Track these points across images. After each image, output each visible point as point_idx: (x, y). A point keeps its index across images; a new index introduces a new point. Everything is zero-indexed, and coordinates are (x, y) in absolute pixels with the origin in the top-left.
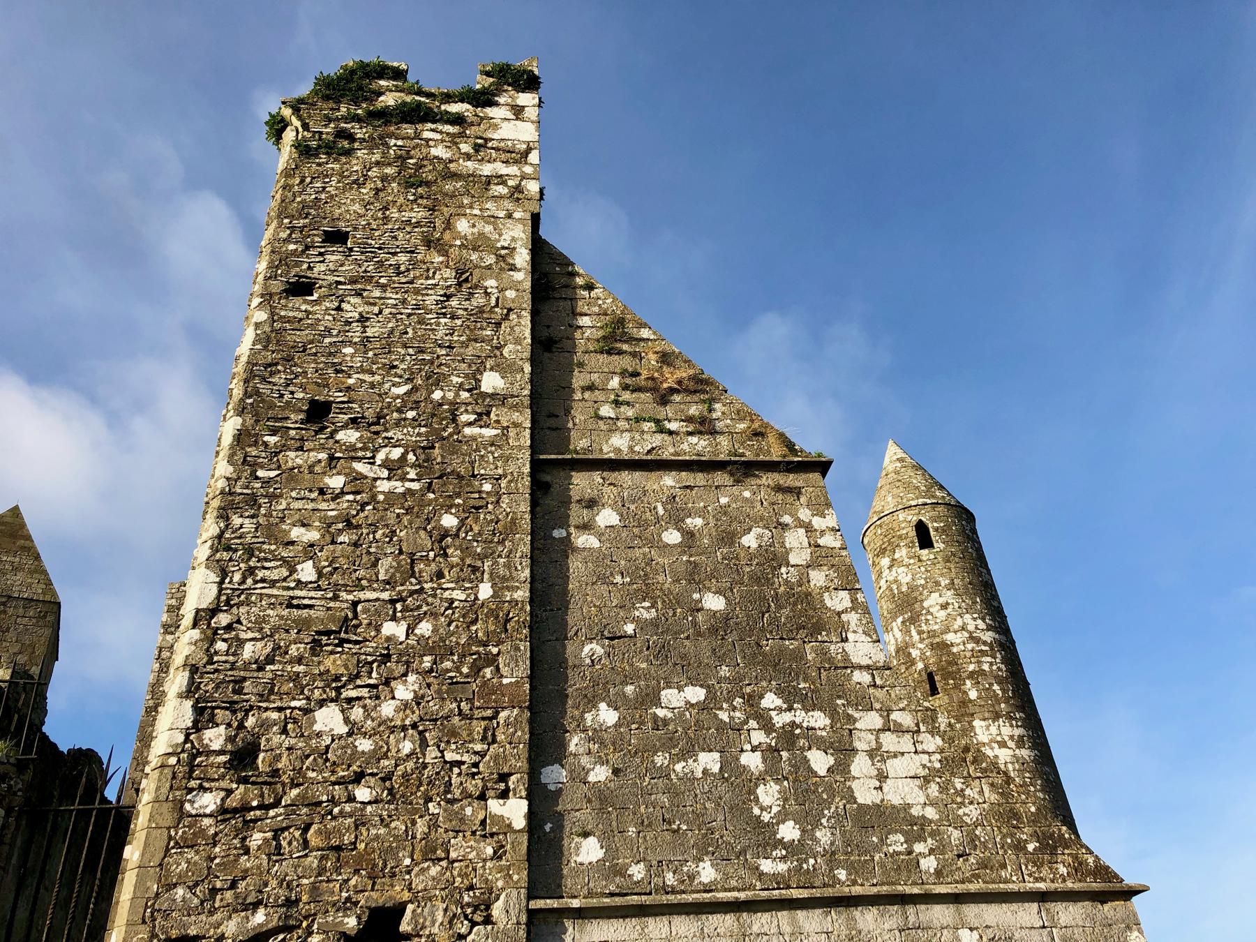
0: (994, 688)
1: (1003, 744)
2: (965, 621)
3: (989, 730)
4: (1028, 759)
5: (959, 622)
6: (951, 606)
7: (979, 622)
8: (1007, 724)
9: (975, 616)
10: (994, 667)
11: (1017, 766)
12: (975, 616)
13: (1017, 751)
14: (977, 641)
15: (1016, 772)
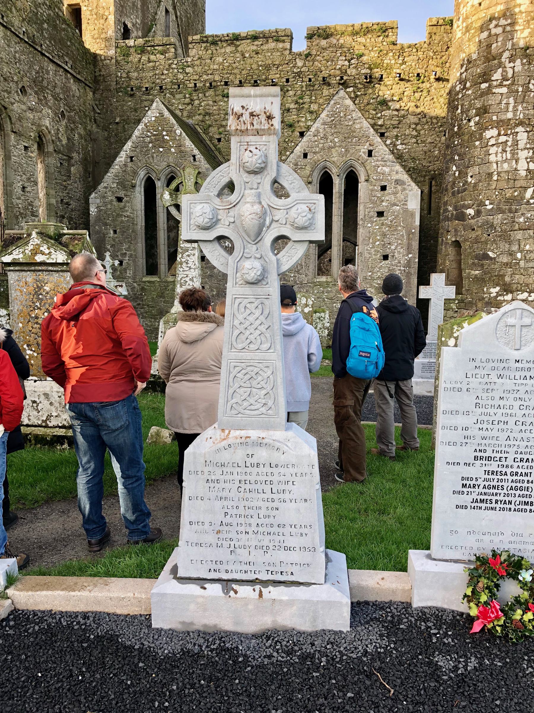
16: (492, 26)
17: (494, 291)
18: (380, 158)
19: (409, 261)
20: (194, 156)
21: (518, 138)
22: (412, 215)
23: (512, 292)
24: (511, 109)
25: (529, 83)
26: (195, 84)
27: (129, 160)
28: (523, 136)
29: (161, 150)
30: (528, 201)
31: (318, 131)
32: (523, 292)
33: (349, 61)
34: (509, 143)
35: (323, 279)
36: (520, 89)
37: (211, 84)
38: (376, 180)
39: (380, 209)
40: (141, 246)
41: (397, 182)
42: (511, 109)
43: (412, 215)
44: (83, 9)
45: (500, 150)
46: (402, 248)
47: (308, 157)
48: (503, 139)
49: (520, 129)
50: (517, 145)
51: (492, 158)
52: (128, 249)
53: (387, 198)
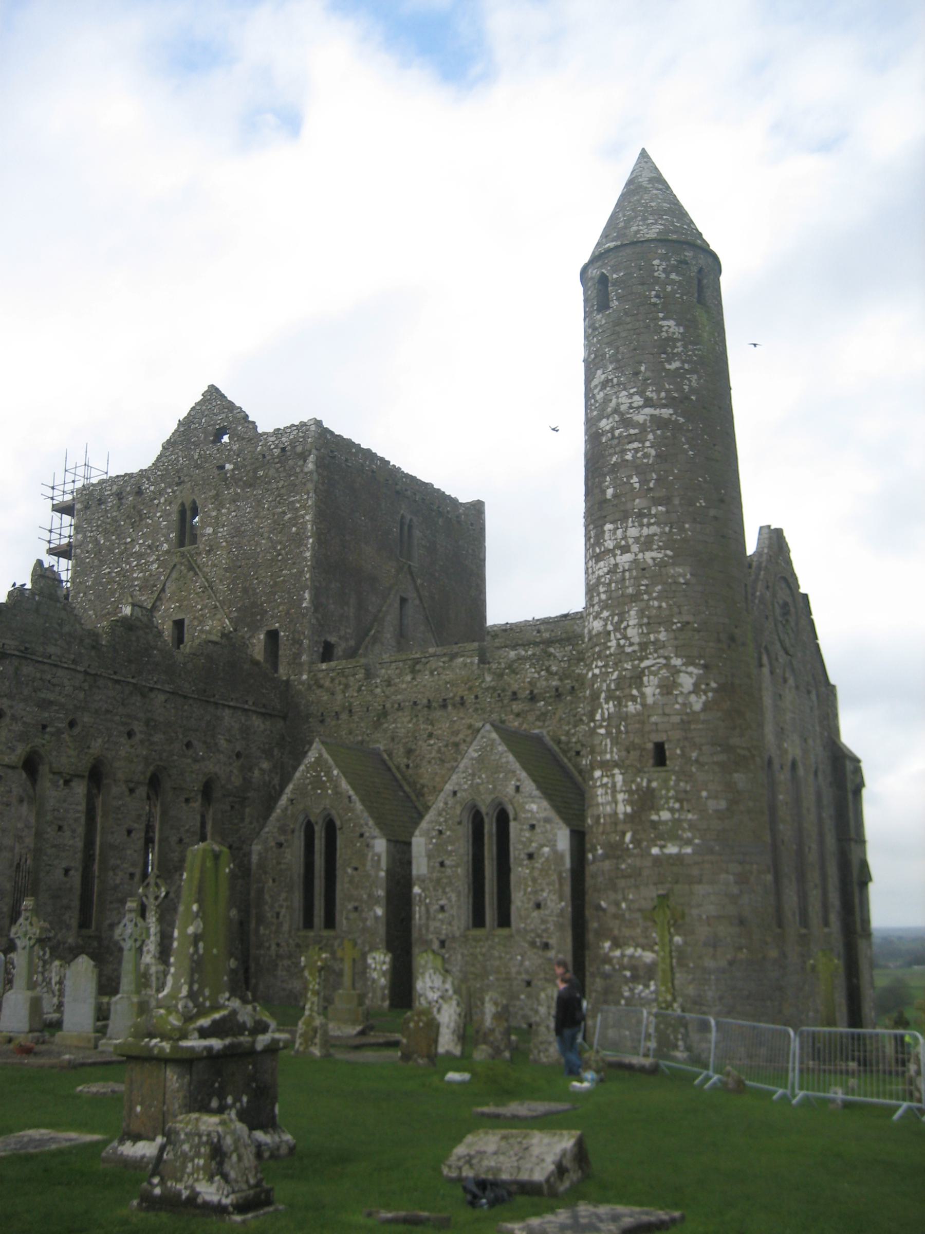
0: (632, 481)
1: (626, 549)
2: (620, 400)
3: (615, 534)
4: (650, 562)
5: (613, 404)
6: (610, 384)
7: (636, 398)
8: (636, 524)
9: (632, 391)
10: (639, 455)
11: (634, 573)
12: (632, 391)
13: (640, 556)
14: (626, 422)
15: (632, 581)
16: (594, 666)
17: (607, 944)
19: (562, 910)
20: (350, 797)
22: (562, 857)
24: (608, 750)
25: (620, 724)
26: (384, 706)
27: (289, 803)
28: (619, 778)
30: (628, 846)
31: (467, 768)
32: (629, 946)
33: (539, 673)
34: (610, 785)
36: (614, 731)
37: (399, 705)
39: (531, 850)
40: (297, 897)
41: (547, 820)
42: (608, 750)
43: (562, 857)
44: (282, 634)
45: (604, 791)
47: (459, 795)
48: (605, 780)
49: (616, 771)
51: (600, 800)
52: (286, 900)
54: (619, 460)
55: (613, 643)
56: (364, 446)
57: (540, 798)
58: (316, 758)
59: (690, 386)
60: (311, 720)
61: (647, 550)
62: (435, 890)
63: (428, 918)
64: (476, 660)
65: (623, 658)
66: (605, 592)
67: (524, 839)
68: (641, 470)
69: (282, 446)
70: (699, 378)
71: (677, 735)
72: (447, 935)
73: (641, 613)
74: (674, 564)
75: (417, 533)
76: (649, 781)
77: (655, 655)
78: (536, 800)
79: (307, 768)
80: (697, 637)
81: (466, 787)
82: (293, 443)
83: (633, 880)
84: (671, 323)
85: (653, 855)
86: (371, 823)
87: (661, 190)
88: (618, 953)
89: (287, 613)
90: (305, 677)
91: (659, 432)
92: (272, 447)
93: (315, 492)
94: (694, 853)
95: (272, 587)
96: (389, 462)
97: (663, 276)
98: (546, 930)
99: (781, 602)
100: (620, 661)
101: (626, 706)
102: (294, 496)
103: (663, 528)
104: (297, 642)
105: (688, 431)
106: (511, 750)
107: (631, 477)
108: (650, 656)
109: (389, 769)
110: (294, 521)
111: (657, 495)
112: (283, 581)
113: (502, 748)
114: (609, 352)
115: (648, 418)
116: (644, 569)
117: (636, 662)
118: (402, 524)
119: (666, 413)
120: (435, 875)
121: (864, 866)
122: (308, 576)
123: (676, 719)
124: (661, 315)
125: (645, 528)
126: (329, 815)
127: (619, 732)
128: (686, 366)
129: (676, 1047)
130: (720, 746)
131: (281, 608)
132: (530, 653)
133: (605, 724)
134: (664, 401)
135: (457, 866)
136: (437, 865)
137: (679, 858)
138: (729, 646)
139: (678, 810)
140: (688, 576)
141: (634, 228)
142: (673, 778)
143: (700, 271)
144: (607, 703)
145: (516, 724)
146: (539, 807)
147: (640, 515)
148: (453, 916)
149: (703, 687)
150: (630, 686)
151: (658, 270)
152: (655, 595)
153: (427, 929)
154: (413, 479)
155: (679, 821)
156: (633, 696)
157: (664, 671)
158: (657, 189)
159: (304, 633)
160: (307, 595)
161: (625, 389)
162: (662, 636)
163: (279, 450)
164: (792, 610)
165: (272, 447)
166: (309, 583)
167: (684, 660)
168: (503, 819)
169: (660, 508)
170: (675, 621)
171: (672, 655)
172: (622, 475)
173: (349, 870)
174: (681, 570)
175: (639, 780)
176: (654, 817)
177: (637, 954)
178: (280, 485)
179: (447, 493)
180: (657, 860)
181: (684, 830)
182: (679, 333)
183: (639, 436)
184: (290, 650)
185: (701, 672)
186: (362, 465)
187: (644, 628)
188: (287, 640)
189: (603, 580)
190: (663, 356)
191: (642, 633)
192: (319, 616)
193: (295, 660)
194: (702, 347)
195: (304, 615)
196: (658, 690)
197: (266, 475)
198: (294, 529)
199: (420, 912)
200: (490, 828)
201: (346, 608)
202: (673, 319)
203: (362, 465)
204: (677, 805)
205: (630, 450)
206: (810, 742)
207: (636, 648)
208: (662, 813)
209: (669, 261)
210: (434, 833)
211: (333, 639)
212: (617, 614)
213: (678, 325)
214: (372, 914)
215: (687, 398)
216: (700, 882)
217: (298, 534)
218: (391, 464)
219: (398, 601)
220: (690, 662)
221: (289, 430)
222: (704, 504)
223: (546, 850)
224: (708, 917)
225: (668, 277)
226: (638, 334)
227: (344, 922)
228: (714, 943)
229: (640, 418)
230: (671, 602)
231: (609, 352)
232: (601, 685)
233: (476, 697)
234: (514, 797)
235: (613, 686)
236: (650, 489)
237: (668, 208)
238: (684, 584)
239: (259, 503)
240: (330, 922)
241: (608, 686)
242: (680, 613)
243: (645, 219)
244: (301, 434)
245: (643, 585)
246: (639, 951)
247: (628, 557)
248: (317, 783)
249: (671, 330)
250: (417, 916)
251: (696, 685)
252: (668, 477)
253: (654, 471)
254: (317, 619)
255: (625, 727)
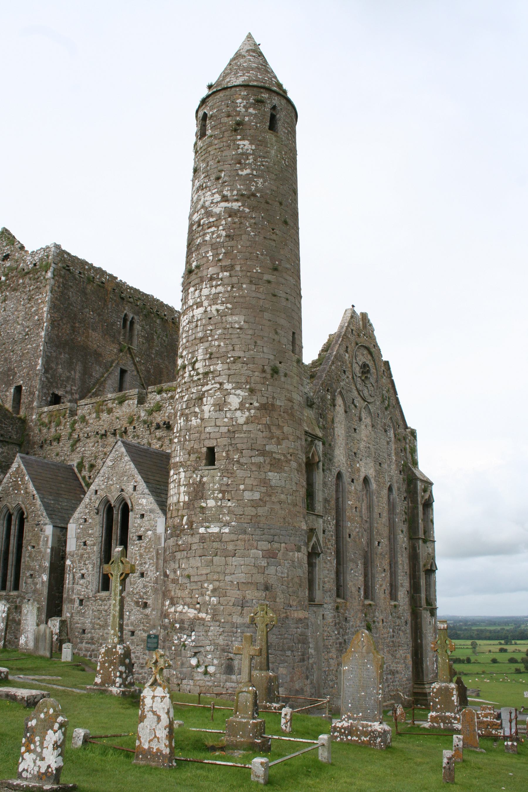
0: (208, 255)
1: (199, 305)
2: (206, 199)
3: (194, 294)
4: (215, 313)
5: (201, 203)
7: (217, 196)
8: (208, 286)
10: (214, 236)
12: (214, 191)
14: (208, 214)
18: (140, 492)
20: (34, 495)
21: (181, 477)
23: (175, 605)
26: (79, 435)
28: (182, 475)
29: (16, 492)
30: (184, 527)
31: (105, 473)
34: (177, 481)
35: (104, 594)
38: (138, 509)
39: (140, 533)
41: (152, 511)
43: (159, 538)
44: (24, 388)
46: (153, 566)
47: (98, 493)
49: (181, 470)
50: (180, 482)
53: (144, 525)
54: (201, 241)
55: (187, 375)
56: (96, 265)
57: (149, 495)
58: (17, 468)
59: (256, 186)
60: (36, 446)
61: (214, 304)
62: (79, 562)
63: (73, 583)
64: (136, 402)
65: (192, 385)
66: (186, 337)
67: (136, 525)
68: (214, 247)
69: (34, 262)
70: (265, 182)
71: (224, 441)
72: (84, 595)
73: (206, 349)
74: (232, 314)
75: (137, 327)
76: (202, 477)
77: (213, 382)
78: (146, 496)
79: (11, 475)
80: (246, 368)
81: (103, 487)
82: (41, 259)
83: (185, 552)
84: (246, 142)
85: (200, 534)
86: (45, 514)
87: (254, 56)
88: (172, 610)
89: (28, 374)
90: (34, 417)
91: (229, 219)
92: (29, 263)
93: (51, 292)
94: (230, 533)
95: (20, 357)
96: (116, 278)
97: (244, 110)
98: (145, 593)
99: (360, 363)
100: (190, 388)
101: (191, 421)
102: (38, 295)
103: (226, 288)
104: (32, 393)
105: (252, 218)
106: (133, 460)
107: (208, 252)
108: (209, 382)
109: (77, 479)
110: (36, 313)
111: (224, 263)
112: (28, 352)
113: (127, 458)
114: (203, 165)
115: (223, 210)
116: (210, 318)
117: (200, 387)
118: (125, 320)
119: (236, 205)
120: (81, 551)
121: (432, 558)
122: (42, 348)
123: (224, 430)
124: (239, 137)
125: (213, 288)
126: (21, 509)
127: (185, 440)
128: (255, 173)
129: (114, 683)
130: (258, 451)
131: (25, 370)
132: (169, 395)
133: (178, 435)
134: (235, 197)
135: (94, 545)
136: (82, 544)
137: (218, 537)
138: (272, 377)
139: (221, 500)
140: (242, 323)
141: (228, 80)
142: (219, 474)
143: (274, 108)
144: (180, 419)
145: (158, 446)
146: (147, 502)
147: (211, 279)
148: (89, 581)
149: (247, 405)
150: (194, 405)
151: (240, 106)
152: (216, 337)
153: (73, 591)
154: (136, 291)
155: (221, 507)
156: (196, 412)
157: (219, 393)
158: (251, 56)
159: (36, 387)
160: (40, 361)
161: (210, 190)
162: (219, 367)
163: (33, 265)
164: (373, 370)
165: (29, 263)
166: (42, 353)
167: (234, 385)
168: (126, 510)
169: (225, 273)
170: (229, 356)
171: (225, 381)
172: (202, 251)
173: (29, 548)
174: (237, 319)
175: (195, 476)
176: (204, 505)
177: (184, 611)
178: (31, 288)
179: (165, 302)
180: (203, 539)
181: (224, 514)
182: (251, 149)
183: (215, 223)
184: (28, 399)
185: (247, 394)
186: (93, 278)
187: (207, 361)
188: (26, 392)
189: (185, 329)
190: (238, 165)
191: (205, 366)
192: (49, 376)
193: (30, 407)
194: (269, 160)
195: (37, 375)
196: (213, 408)
197: (23, 283)
198: (36, 317)
199: (69, 579)
200: (117, 516)
201: (73, 373)
202: (247, 140)
203: (93, 278)
204: (220, 496)
205: (208, 233)
206: (385, 466)
207: (201, 376)
208: (208, 501)
209: (249, 100)
210: (82, 521)
211: (60, 393)
212: (190, 353)
213: (251, 144)
214: (40, 579)
215: (254, 195)
216: (234, 556)
217: (38, 320)
218: (119, 279)
219: (119, 371)
220: (238, 386)
221: (39, 252)
222: (259, 271)
223: (150, 533)
224: (238, 583)
225: (246, 111)
226: (222, 151)
227: (24, 585)
228: (243, 604)
229: (217, 210)
230: (227, 342)
231: (203, 165)
232: (178, 407)
233: (134, 428)
234: (132, 494)
235: (184, 407)
236: (220, 260)
237: (256, 67)
238: (238, 328)
239: (19, 301)
240: (16, 587)
241: (182, 406)
242: (234, 350)
243: (236, 73)
244: (46, 254)
245: (209, 330)
246: (186, 607)
247: (201, 310)
248: (16, 487)
249: (246, 147)
250: (67, 582)
251: (242, 404)
252: (233, 251)
253: (223, 247)
254: (47, 378)
255: (189, 436)
